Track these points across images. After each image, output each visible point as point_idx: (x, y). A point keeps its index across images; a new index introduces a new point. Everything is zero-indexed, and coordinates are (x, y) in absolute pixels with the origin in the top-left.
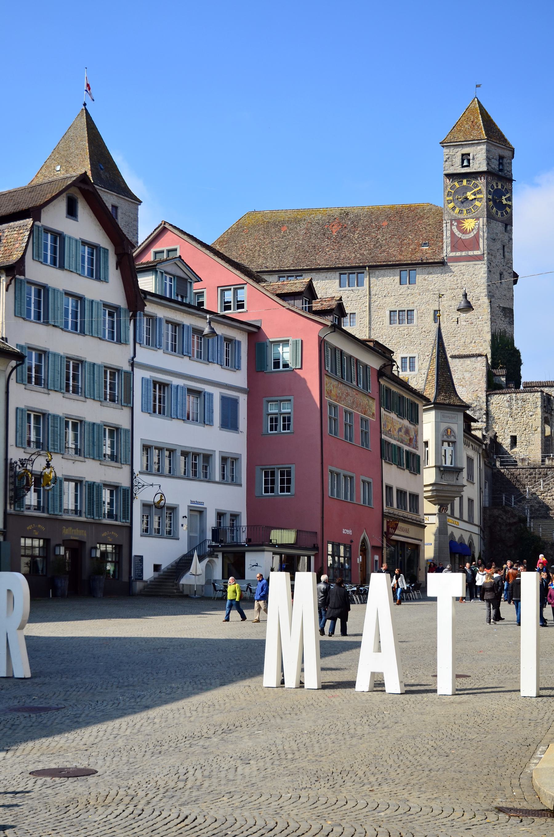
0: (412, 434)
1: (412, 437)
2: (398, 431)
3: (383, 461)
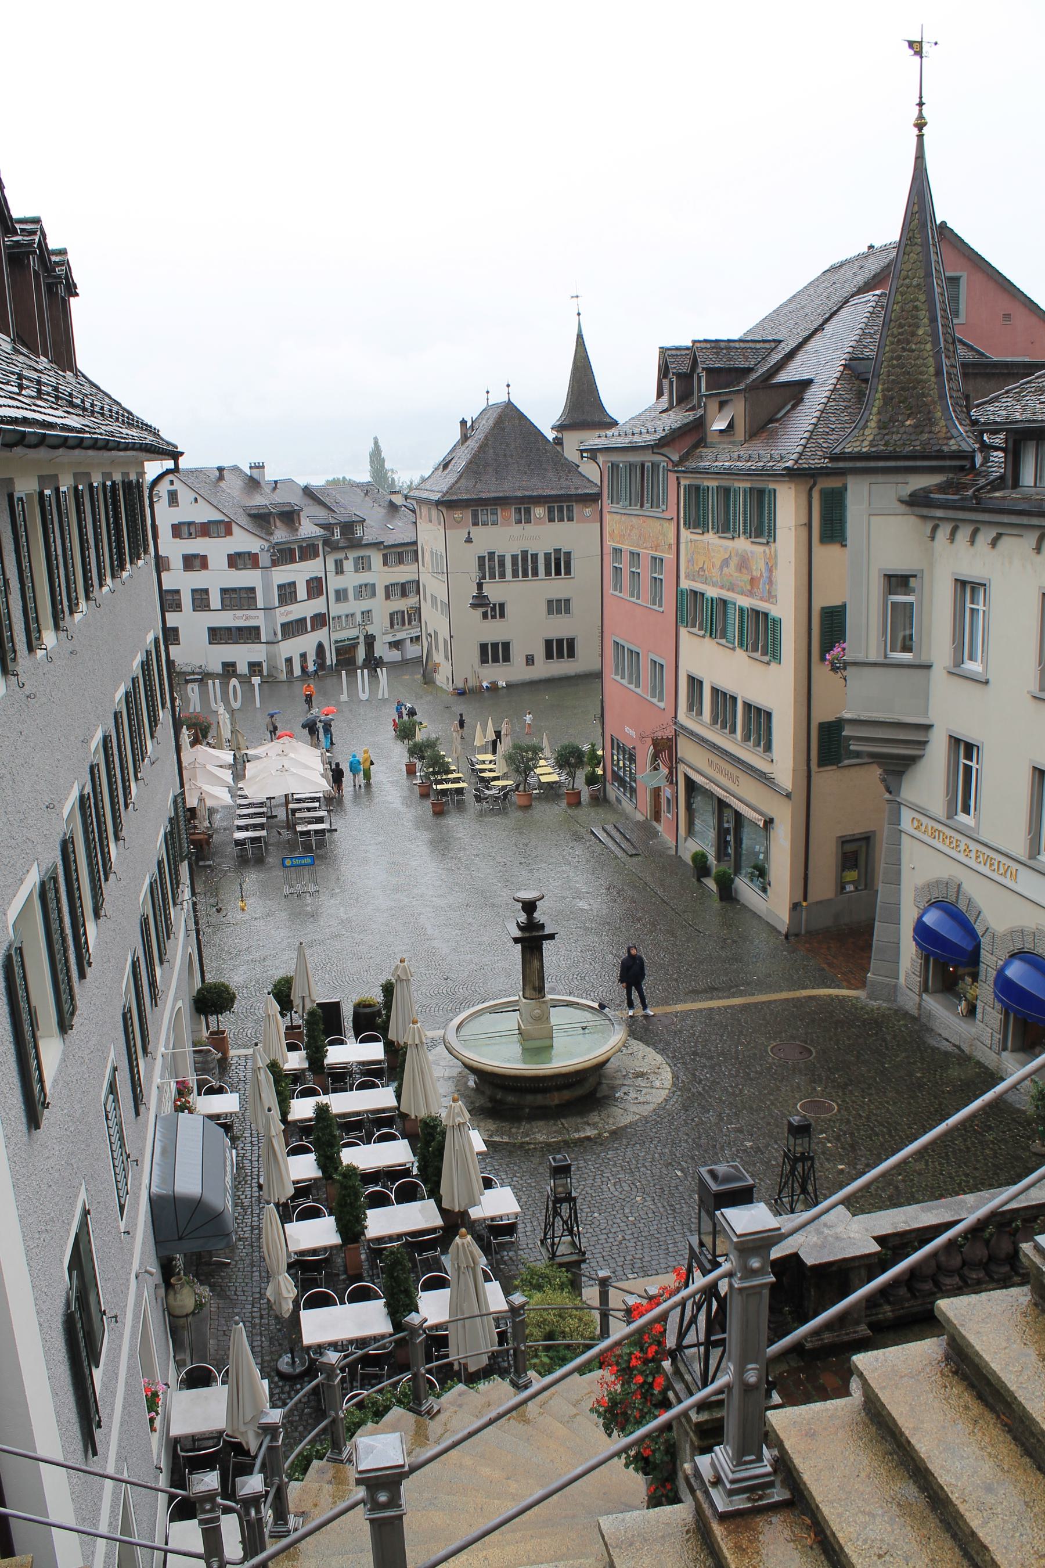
0: (758, 567)
2: (721, 568)
3: (683, 631)
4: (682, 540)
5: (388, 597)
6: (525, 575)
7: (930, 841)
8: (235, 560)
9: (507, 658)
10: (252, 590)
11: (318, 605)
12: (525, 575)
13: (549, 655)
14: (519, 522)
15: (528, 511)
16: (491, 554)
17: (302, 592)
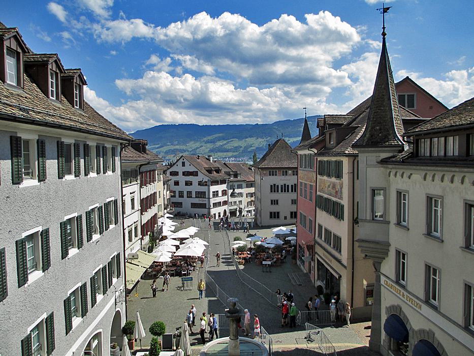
1: (337, 190)
3: (317, 209)
4: (318, 178)
5: (247, 197)
6: (285, 191)
7: (390, 289)
8: (200, 184)
9: (278, 217)
10: (205, 192)
11: (225, 198)
12: (285, 191)
13: (291, 217)
14: (283, 175)
15: (286, 172)
16: (275, 185)
17: (220, 194)
